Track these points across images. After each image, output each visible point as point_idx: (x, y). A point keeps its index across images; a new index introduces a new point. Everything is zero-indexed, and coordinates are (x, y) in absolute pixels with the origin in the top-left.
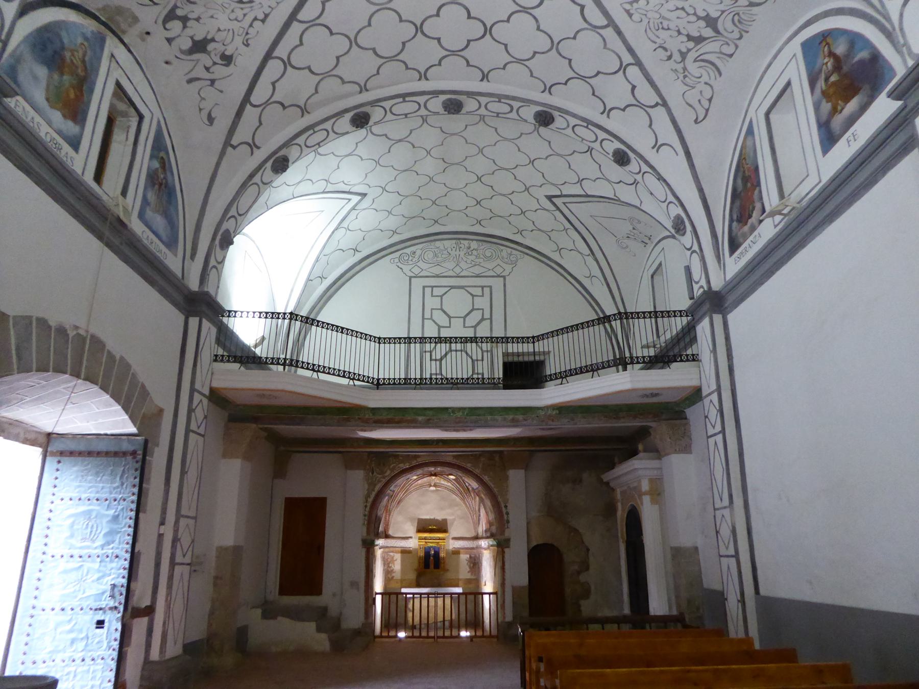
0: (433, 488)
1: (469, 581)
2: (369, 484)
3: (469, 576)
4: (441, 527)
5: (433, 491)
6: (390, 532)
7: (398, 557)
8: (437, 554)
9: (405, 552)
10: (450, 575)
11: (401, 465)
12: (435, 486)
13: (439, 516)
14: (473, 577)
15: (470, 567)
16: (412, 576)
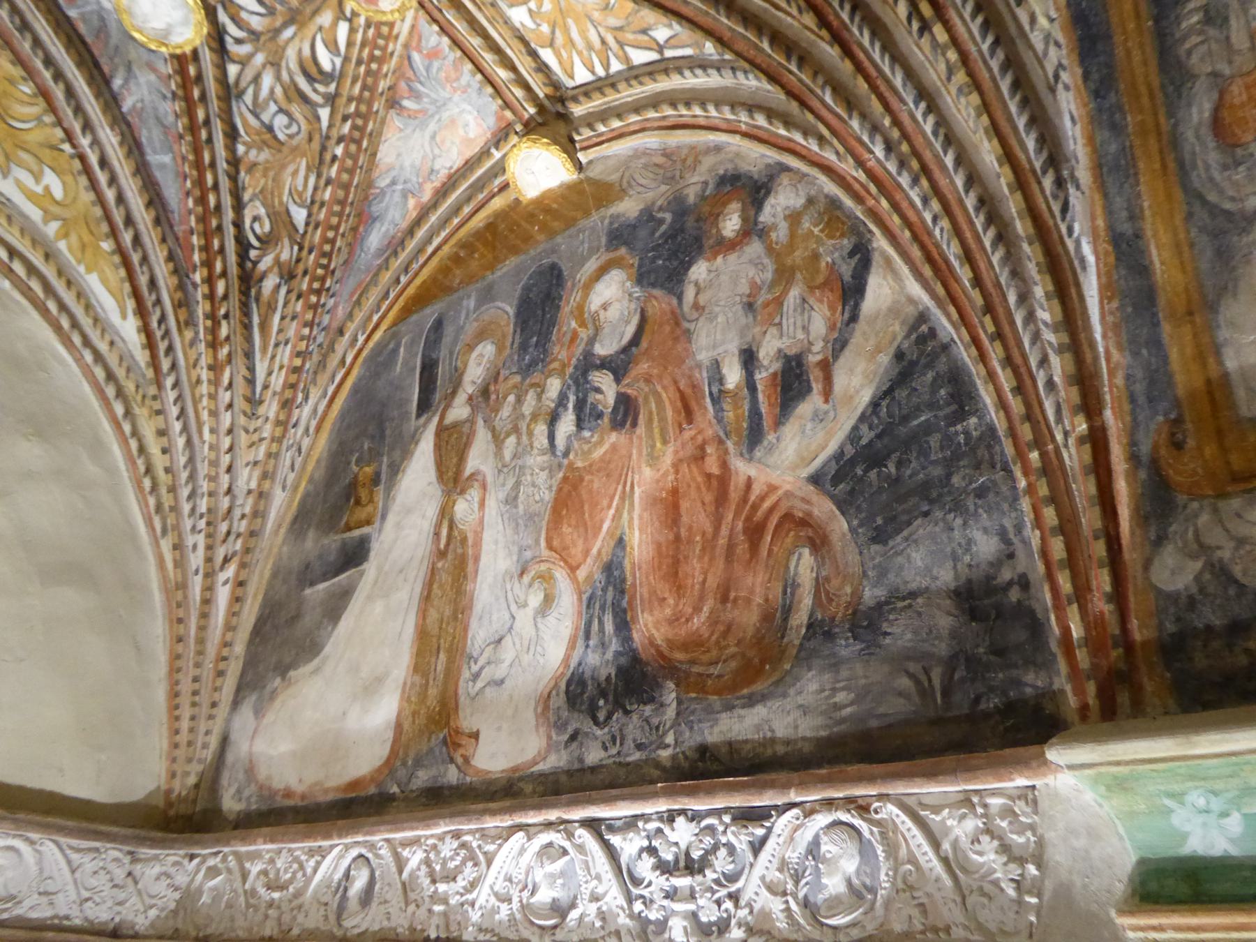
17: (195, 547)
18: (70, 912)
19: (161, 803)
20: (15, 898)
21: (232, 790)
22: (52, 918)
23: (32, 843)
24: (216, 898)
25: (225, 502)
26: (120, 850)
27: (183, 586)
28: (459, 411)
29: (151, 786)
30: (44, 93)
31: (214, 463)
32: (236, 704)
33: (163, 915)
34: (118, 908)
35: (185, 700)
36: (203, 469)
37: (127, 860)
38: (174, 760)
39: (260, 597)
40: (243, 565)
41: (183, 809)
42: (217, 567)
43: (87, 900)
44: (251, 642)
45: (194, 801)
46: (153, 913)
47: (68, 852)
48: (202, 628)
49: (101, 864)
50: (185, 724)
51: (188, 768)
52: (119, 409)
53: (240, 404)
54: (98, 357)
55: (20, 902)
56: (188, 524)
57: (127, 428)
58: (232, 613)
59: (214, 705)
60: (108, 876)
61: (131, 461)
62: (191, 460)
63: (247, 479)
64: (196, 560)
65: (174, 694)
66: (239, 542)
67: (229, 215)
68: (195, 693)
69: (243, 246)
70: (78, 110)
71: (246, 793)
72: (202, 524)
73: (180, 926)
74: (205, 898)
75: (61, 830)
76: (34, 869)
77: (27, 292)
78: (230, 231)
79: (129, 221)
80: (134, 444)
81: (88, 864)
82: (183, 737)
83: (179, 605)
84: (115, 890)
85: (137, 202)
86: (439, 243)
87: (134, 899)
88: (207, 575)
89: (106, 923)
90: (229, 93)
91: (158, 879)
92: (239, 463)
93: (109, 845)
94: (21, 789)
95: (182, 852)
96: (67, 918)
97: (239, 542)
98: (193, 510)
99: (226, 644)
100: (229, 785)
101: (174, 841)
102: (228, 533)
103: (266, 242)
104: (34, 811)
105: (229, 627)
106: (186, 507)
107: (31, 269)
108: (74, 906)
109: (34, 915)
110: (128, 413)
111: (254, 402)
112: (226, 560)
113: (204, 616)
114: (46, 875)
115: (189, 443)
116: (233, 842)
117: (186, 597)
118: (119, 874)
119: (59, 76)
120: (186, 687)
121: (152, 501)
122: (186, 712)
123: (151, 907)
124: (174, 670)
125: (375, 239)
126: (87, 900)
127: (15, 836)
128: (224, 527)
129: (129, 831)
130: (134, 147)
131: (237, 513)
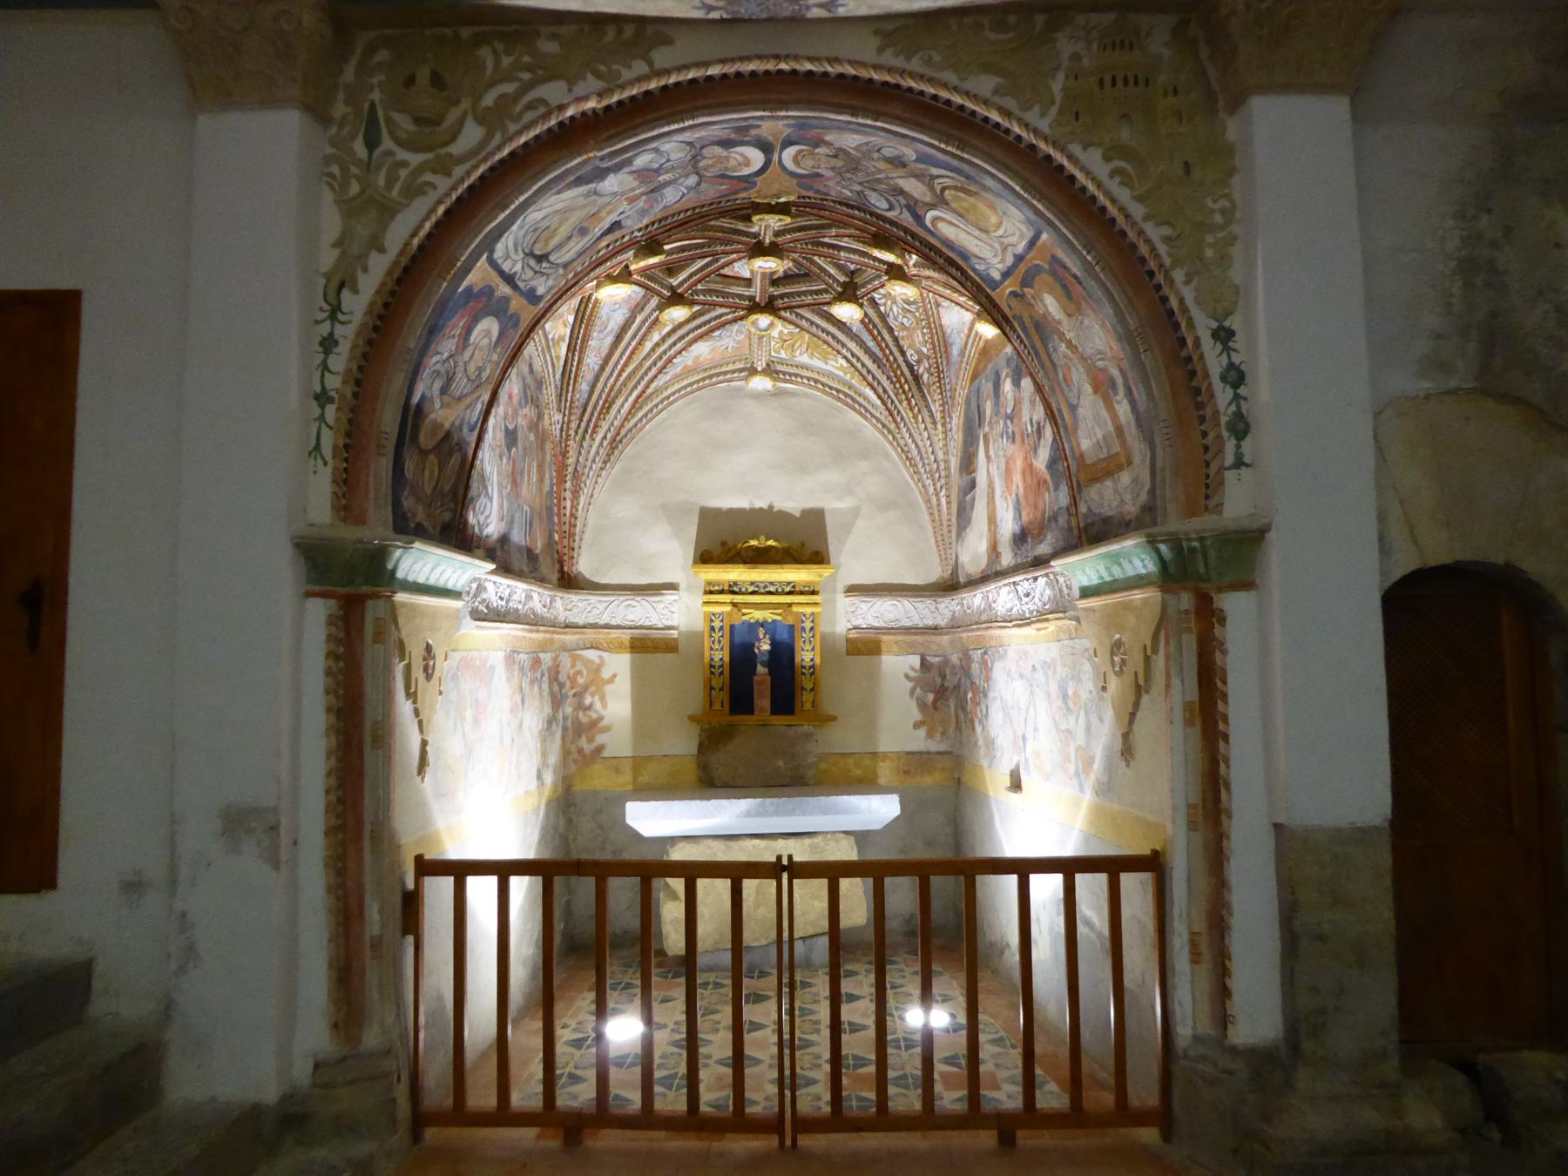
0: (761, 383)
1: (915, 763)
2: (351, 210)
3: (918, 741)
4: (801, 542)
5: (759, 396)
6: (584, 565)
7: (619, 666)
8: (783, 655)
9: (647, 645)
10: (840, 739)
11: (553, 91)
12: (770, 371)
13: (790, 497)
14: (934, 746)
15: (922, 706)
16: (681, 743)
28: (987, 429)
30: (825, 342)
53: (930, 426)
54: (878, 420)
64: (931, 489)
67: (900, 359)
69: (910, 367)
70: (839, 341)
77: (846, 404)
78: (903, 365)
79: (869, 372)
81: (920, 606)
85: (869, 363)
86: (973, 352)
90: (883, 317)
103: (919, 362)
107: (846, 395)
111: (934, 423)
119: (828, 333)
125: (955, 351)
130: (861, 344)
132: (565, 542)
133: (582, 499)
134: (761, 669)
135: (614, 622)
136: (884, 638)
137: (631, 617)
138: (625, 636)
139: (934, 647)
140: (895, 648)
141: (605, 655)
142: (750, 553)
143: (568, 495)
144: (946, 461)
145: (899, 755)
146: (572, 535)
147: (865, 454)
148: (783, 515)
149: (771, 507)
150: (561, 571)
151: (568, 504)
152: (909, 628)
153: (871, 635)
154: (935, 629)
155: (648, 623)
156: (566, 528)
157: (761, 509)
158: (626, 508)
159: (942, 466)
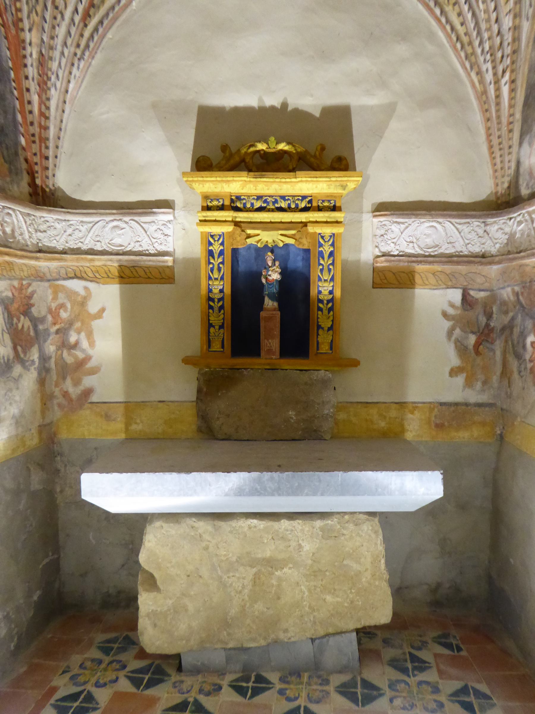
1: (450, 415)
3: (455, 391)
4: (321, 144)
6: (64, 178)
7: (107, 297)
8: (295, 287)
9: (138, 274)
10: (362, 386)
13: (308, 91)
14: (473, 396)
15: (461, 349)
16: (179, 387)
17: (487, 70)
18: (462, 249)
19: (493, 198)
20: (438, 245)
21: (525, 184)
22: (455, 252)
23: (440, 223)
24: (522, 235)
25: (498, 40)
26: (479, 222)
27: (485, 92)
29: (488, 192)
31: (488, 20)
32: (521, 144)
33: (502, 246)
34: (483, 246)
35: (496, 149)
36: (483, 26)
37: (483, 225)
38: (496, 178)
39: (525, 85)
40: (512, 71)
41: (504, 199)
42: (500, 77)
43: (468, 244)
44: (523, 111)
45: (509, 195)
46: (498, 246)
47: (456, 225)
48: (498, 111)
49: (472, 228)
50: (498, 160)
51: (503, 180)
52: (438, 11)
55: (441, 247)
56: (482, 59)
57: (443, 20)
58: (511, 99)
59: (510, 147)
60: (476, 233)
61: (449, 37)
62: (477, 24)
63: (507, 22)
64: (489, 77)
65: (491, 147)
66: (509, 58)
68: (500, 144)
71: (531, 184)
72: (488, 57)
73: (510, 249)
74: (518, 235)
75: (450, 216)
76: (443, 234)
80: (448, 28)
81: (465, 229)
82: (499, 166)
83: (485, 103)
84: (480, 238)
87: (489, 241)
88: (495, 83)
89: (479, 252)
91: (497, 231)
92: (502, 15)
93: (473, 220)
94: (431, 202)
95: (505, 218)
96: (461, 252)
97: (509, 58)
98: (483, 51)
99: (511, 115)
100: (523, 183)
101: (502, 213)
102: (503, 57)
104: (439, 210)
105: (511, 106)
106: (479, 51)
108: (463, 247)
109: (447, 252)
110: (442, 12)
112: (504, 72)
113: (498, 104)
114: (449, 235)
115: (474, 15)
116: (525, 207)
117: (487, 98)
118: (481, 232)
120: (495, 142)
121: (463, 54)
122: (498, 154)
123: (496, 243)
124: (489, 135)
126: (468, 244)
127: (432, 221)
128: (499, 55)
129: (481, 213)
131: (505, 44)
132: (35, 148)
133: (54, 94)
134: (269, 303)
135: (98, 247)
136: (420, 268)
137: (118, 241)
138: (112, 264)
139: (480, 280)
140: (432, 280)
141: (91, 286)
142: (258, 160)
143: (33, 86)
144: (516, 28)
145: (431, 406)
146: (44, 140)
147: (404, 35)
148: (300, 115)
149: (285, 105)
150: (32, 184)
151: (35, 99)
152: (450, 256)
153: (403, 264)
154: (483, 258)
155: (137, 248)
156: (35, 129)
157: (273, 108)
158: (109, 109)
159: (508, 37)
